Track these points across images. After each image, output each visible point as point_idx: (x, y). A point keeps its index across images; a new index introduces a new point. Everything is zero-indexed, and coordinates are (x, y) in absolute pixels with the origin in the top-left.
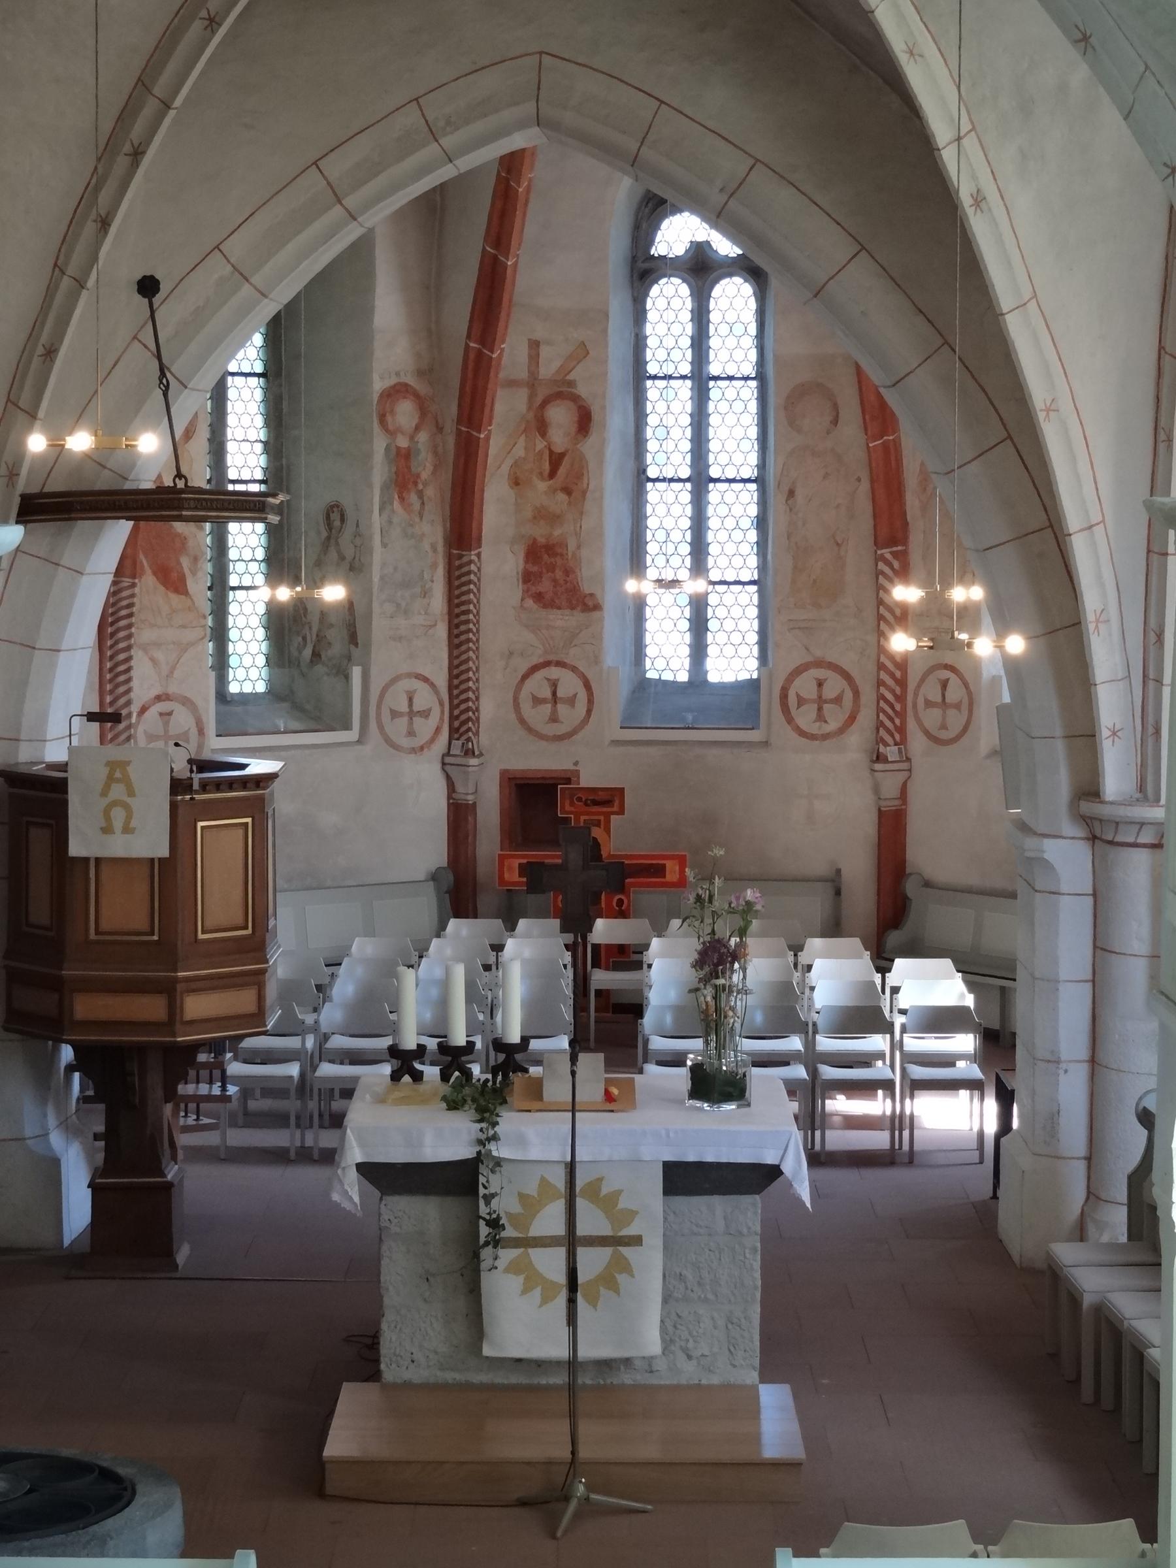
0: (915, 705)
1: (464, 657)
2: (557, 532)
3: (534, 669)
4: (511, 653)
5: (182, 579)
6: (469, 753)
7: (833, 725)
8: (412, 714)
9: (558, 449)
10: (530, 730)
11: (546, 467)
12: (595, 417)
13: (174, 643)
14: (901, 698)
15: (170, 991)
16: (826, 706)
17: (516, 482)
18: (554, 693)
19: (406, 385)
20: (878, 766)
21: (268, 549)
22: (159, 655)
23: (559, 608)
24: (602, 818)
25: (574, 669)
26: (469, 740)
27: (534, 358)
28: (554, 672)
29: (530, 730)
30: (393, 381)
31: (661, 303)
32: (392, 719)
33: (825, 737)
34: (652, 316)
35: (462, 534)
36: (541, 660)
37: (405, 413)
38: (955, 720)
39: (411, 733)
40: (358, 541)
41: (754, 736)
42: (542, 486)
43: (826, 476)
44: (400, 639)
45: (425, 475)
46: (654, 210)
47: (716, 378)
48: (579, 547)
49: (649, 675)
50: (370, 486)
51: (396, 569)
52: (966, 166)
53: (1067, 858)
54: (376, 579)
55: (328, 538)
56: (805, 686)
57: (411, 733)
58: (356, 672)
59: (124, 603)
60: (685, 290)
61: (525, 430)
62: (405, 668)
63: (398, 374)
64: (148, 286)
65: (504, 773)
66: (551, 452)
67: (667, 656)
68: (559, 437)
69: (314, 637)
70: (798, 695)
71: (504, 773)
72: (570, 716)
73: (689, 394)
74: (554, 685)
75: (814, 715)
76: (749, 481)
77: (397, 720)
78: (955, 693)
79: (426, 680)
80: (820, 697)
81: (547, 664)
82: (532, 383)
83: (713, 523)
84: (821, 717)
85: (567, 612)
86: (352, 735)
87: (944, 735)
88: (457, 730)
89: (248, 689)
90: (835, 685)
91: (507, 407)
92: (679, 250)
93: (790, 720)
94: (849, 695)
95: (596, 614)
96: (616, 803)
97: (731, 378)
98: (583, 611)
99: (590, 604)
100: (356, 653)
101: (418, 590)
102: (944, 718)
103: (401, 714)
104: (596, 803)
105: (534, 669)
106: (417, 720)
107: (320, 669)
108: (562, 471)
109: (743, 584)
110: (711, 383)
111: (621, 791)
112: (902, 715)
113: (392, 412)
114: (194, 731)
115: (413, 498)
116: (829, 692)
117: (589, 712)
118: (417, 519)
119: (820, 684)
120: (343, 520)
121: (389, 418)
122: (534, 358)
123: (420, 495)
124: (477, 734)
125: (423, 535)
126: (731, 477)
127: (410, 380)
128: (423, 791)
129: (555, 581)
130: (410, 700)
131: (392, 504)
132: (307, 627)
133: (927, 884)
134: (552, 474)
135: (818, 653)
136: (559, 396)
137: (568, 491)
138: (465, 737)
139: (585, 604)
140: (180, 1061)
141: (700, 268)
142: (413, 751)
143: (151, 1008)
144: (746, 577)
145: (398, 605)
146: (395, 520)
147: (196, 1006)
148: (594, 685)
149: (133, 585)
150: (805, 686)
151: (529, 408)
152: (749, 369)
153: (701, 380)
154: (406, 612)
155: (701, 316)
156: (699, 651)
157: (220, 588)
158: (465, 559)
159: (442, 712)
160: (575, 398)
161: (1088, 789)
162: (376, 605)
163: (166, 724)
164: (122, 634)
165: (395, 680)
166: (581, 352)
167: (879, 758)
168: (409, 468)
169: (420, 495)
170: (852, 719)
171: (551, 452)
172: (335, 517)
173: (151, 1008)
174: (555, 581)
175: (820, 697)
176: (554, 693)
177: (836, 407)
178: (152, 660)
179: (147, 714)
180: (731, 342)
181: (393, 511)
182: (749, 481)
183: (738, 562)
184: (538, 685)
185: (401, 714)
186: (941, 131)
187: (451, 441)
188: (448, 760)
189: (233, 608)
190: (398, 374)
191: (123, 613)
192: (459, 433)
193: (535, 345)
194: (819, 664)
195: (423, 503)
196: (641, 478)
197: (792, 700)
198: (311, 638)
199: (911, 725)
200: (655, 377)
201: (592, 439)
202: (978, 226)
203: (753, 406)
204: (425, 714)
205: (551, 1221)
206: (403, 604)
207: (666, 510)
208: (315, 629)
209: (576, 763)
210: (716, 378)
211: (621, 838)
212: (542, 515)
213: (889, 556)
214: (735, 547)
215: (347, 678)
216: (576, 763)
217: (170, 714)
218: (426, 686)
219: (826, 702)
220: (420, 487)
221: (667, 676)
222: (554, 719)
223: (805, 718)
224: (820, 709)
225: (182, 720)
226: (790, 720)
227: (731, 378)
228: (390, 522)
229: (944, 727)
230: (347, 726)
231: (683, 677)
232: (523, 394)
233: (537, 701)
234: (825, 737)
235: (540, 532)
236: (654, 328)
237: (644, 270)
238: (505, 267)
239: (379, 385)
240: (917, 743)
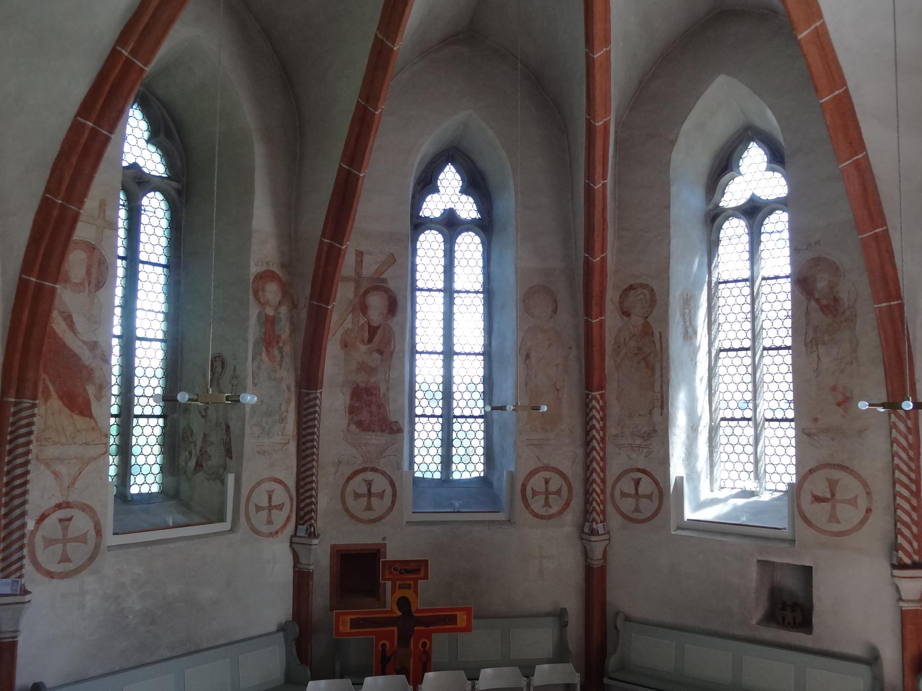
0: (612, 496)
1: (309, 466)
2: (373, 380)
3: (356, 473)
4: (340, 462)
5: (88, 404)
6: (312, 535)
7: (555, 509)
8: (271, 508)
9: (375, 324)
10: (352, 516)
11: (366, 335)
12: (400, 303)
13: (76, 458)
14: (603, 491)
16: (550, 496)
17: (345, 345)
18: (369, 490)
19: (273, 272)
20: (593, 538)
21: (165, 389)
22: (61, 469)
23: (374, 431)
24: (412, 582)
25: (383, 473)
26: (311, 525)
27: (359, 263)
28: (369, 475)
29: (352, 516)
30: (264, 268)
31: (426, 245)
32: (257, 512)
33: (550, 517)
34: (420, 252)
35: (309, 379)
36: (361, 467)
37: (272, 291)
38: (648, 507)
39: (270, 522)
40: (235, 382)
41: (501, 516)
42: (363, 348)
43: (550, 345)
44: (264, 453)
45: (285, 336)
46: (422, 189)
47: (459, 292)
48: (388, 390)
49: (416, 475)
50: (246, 340)
56: (537, 482)
57: (270, 522)
58: (231, 478)
59: (24, 422)
60: (440, 238)
61: (352, 311)
62: (266, 474)
63: (268, 263)
65: (333, 547)
66: (370, 326)
67: (426, 462)
69: (198, 452)
70: (532, 489)
71: (333, 547)
72: (379, 506)
73: (442, 300)
74: (369, 484)
75: (543, 502)
76: (479, 354)
77: (261, 513)
78: (646, 486)
79: (281, 482)
80: (547, 490)
81: (364, 470)
82: (358, 278)
83: (456, 380)
84: (547, 504)
85: (379, 434)
86: (225, 526)
87: (636, 516)
88: (302, 518)
89: (145, 489)
90: (556, 483)
91: (344, 293)
92: (437, 214)
93: (527, 506)
94: (565, 488)
95: (398, 436)
96: (422, 572)
97: (468, 292)
98: (390, 433)
99: (395, 428)
101: (277, 418)
102: (637, 505)
103: (263, 509)
104: (408, 571)
105: (356, 473)
106: (275, 512)
107: (201, 475)
108: (377, 338)
109: (475, 417)
110: (456, 295)
111: (426, 562)
112: (603, 502)
113: (263, 290)
114: (92, 532)
115: (276, 352)
116: (553, 487)
117: (393, 502)
118: (278, 367)
119: (547, 482)
120: (223, 366)
121: (260, 293)
122: (359, 263)
123: (281, 350)
124: (316, 521)
125: (282, 378)
126: (467, 351)
127: (276, 270)
128: (275, 561)
129: (371, 412)
130: (270, 498)
131: (261, 355)
132: (193, 445)
133: (627, 619)
134: (370, 341)
135: (546, 461)
136: (376, 288)
137: (381, 352)
138: (308, 523)
139: (391, 428)
141: (450, 225)
142: (271, 535)
144: (477, 412)
145: (263, 428)
146: (263, 367)
148: (397, 484)
149: (34, 406)
150: (537, 482)
151: (355, 296)
152: (479, 287)
153: (449, 292)
155: (449, 254)
156: (447, 461)
157: (126, 417)
158: (312, 396)
159: (292, 506)
160: (387, 291)
162: (247, 427)
163: (65, 529)
164: (20, 451)
165: (259, 484)
166: (391, 260)
167: (593, 532)
168: (273, 330)
169: (281, 350)
170: (567, 505)
171: (370, 326)
174: (371, 412)
175: (547, 490)
176: (369, 490)
177: (555, 302)
178: (55, 473)
179: (46, 521)
180: (468, 270)
181: (262, 360)
182: (479, 354)
183: (472, 404)
184: (358, 484)
185: (263, 509)
187: (304, 314)
188: (295, 540)
189: (136, 431)
190: (268, 263)
191: (23, 431)
192: (311, 305)
193: (360, 254)
194: (546, 468)
195: (282, 357)
197: (529, 493)
198: (196, 452)
199: (610, 508)
200: (422, 290)
201: (397, 318)
203: (481, 309)
204: (280, 507)
208: (198, 448)
209: (384, 539)
210: (459, 292)
211: (427, 596)
212: (363, 368)
213: (598, 397)
215: (223, 482)
216: (384, 539)
217: (70, 519)
218: (281, 487)
219: (551, 493)
220: (281, 345)
221: (428, 475)
222: (369, 508)
223: (537, 505)
224: (547, 498)
225: (81, 523)
226: (527, 506)
227: (468, 292)
228: (259, 368)
229: (637, 510)
230: (222, 519)
231: (437, 476)
232: (351, 286)
233: (357, 496)
234: (550, 517)
235: (361, 379)
238: (358, 177)
239: (254, 270)
240: (615, 521)
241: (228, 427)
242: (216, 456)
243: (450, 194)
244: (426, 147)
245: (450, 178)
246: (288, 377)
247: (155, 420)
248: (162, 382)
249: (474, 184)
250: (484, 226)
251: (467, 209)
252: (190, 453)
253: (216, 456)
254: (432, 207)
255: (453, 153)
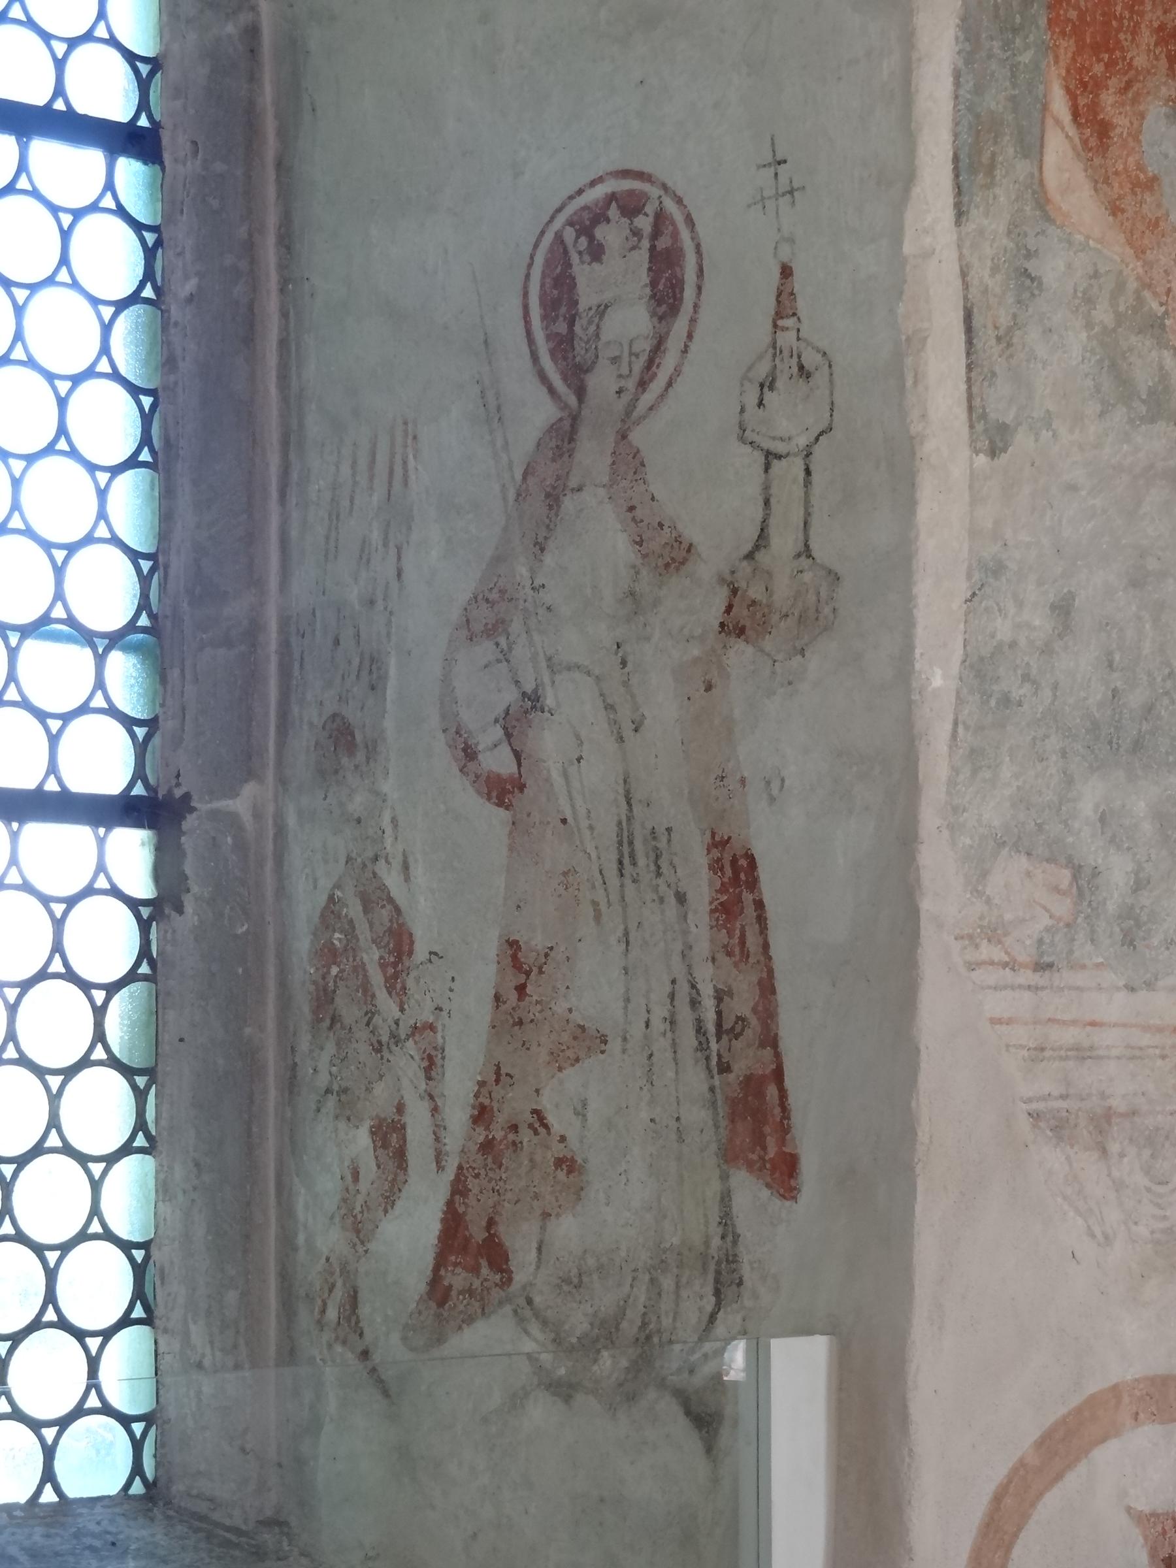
40: (789, 418)
51: (1063, 609)
54: (938, 677)
55: (564, 437)
69: (457, 1117)
100: (778, 1235)
107: (493, 1341)
120: (666, 296)
131: (1033, 149)
132: (406, 1062)
145: (1085, 881)
146: (1055, 268)
154: (1132, 931)
162: (939, 862)
172: (616, 286)
181: (1042, 201)
198: (442, 1125)
206: (1118, 871)
228: (1026, 281)
241: (737, 873)
242: (630, 1169)
247: (77, 838)
248: (130, 506)
252: (390, 1136)
253: (630, 1169)
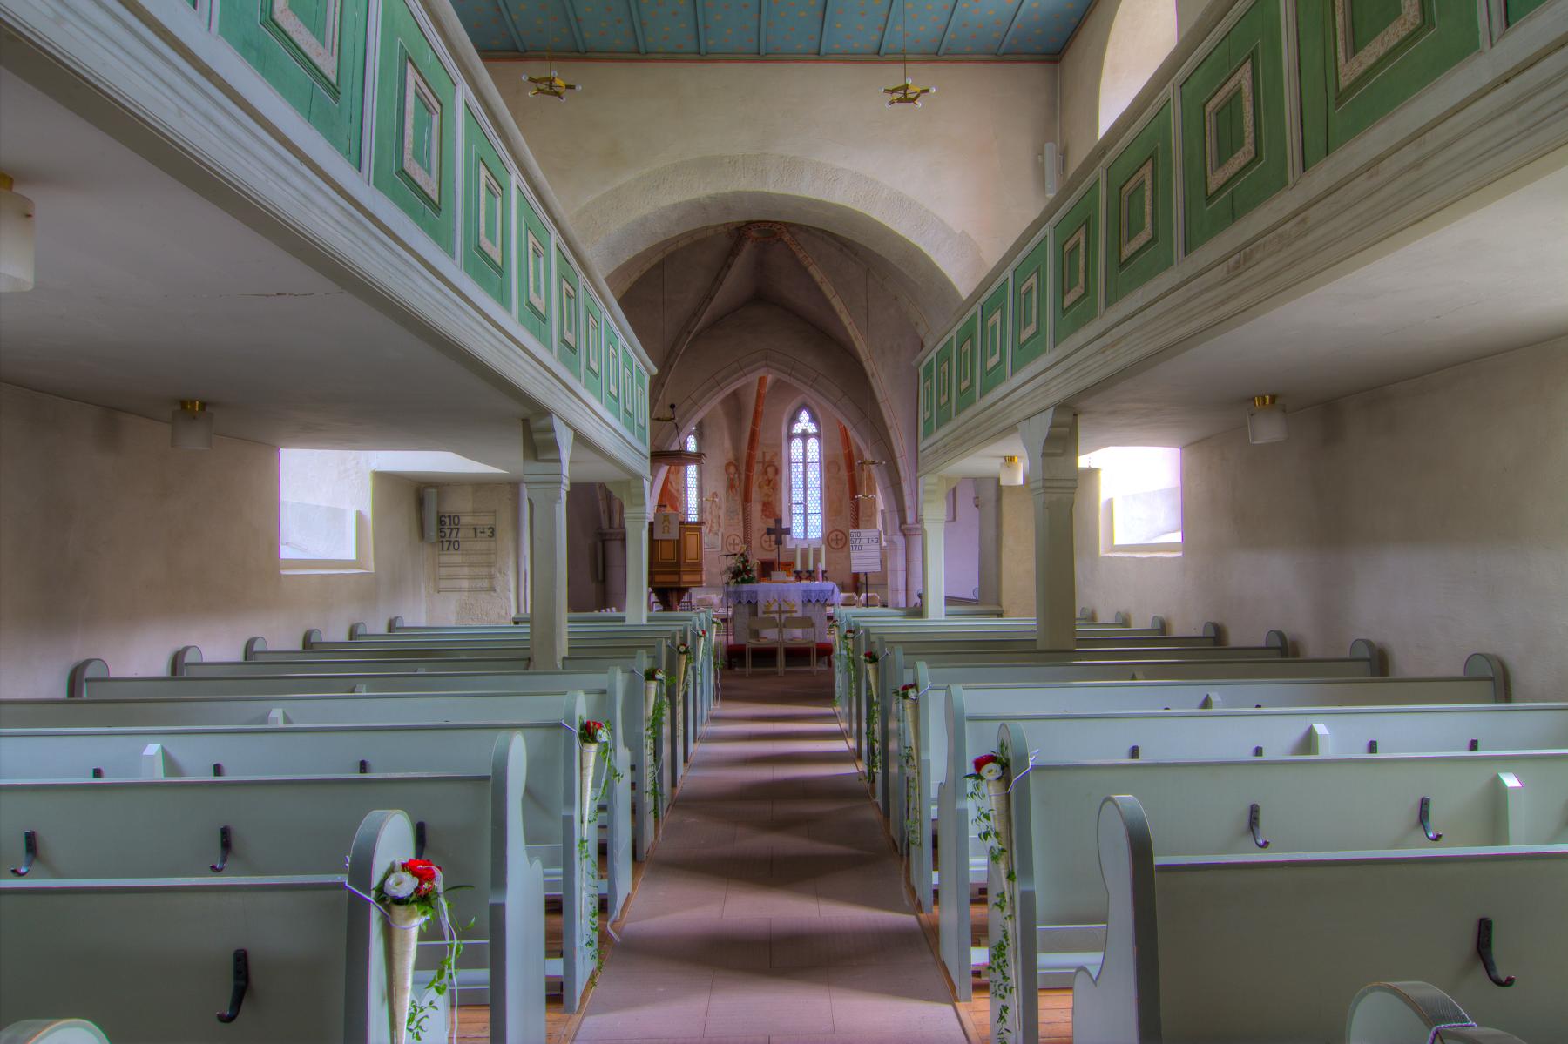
15: (679, 573)
35: (746, 499)
52: (870, 367)
53: (900, 540)
56: (833, 536)
64: (672, 406)
67: (797, 530)
68: (771, 475)
91: (757, 468)
140: (682, 591)
141: (805, 436)
143: (674, 578)
147: (686, 578)
153: (805, 463)
161: (903, 521)
173: (674, 578)
186: (863, 358)
196: (790, 488)
202: (873, 382)
205: (774, 607)
207: (797, 496)
212: (767, 495)
214: (815, 505)
236: (794, 451)
237: (791, 437)
243: (804, 423)
244: (790, 408)
245: (804, 416)
246: (739, 499)
249: (814, 418)
250: (817, 436)
251: (812, 428)
254: (798, 428)
255: (804, 406)
